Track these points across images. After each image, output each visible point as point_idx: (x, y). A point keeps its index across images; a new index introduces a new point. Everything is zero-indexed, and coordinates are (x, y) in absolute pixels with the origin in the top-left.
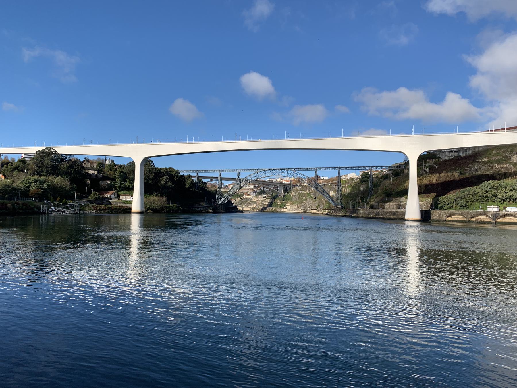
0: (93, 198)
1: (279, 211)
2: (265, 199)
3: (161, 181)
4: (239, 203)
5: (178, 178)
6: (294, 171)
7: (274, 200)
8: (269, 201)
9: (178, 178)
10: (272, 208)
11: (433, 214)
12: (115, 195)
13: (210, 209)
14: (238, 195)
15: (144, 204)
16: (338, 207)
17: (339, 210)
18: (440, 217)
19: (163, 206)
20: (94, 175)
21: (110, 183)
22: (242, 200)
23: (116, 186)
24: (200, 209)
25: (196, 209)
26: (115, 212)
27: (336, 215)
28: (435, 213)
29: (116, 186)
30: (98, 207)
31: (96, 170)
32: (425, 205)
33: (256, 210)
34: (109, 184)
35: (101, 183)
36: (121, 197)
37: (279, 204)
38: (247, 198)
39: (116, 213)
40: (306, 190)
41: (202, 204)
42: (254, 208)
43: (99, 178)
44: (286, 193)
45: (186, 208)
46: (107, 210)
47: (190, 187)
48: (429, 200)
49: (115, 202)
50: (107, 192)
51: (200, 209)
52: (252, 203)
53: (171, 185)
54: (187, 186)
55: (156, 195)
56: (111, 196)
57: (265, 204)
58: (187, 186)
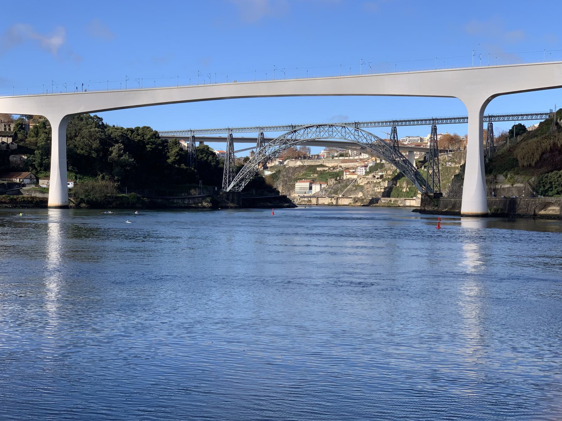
1: (401, 205)
2: (381, 180)
3: (112, 152)
4: (333, 191)
5: (154, 146)
7: (396, 183)
8: (386, 186)
9: (154, 146)
10: (389, 199)
11: (519, 205)
12: (31, 178)
13: (207, 202)
14: (336, 173)
15: (69, 193)
16: (429, 196)
17: (429, 200)
18: (527, 211)
19: (110, 197)
20: (5, 144)
21: (26, 158)
22: (340, 183)
23: (34, 163)
24: (186, 202)
25: (180, 201)
27: (425, 210)
28: (522, 202)
29: (34, 163)
31: (10, 136)
32: (525, 189)
33: (359, 204)
34: (24, 161)
35: (12, 158)
36: (41, 181)
37: (404, 190)
38: (348, 179)
39: (33, 207)
41: (193, 192)
42: (356, 200)
44: (421, 167)
45: (159, 200)
46: (8, 203)
47: (179, 162)
48: (533, 179)
49: (28, 191)
50: (19, 173)
51: (186, 202)
54: (169, 161)
55: (103, 178)
56: (25, 180)
57: (379, 191)
58: (169, 161)
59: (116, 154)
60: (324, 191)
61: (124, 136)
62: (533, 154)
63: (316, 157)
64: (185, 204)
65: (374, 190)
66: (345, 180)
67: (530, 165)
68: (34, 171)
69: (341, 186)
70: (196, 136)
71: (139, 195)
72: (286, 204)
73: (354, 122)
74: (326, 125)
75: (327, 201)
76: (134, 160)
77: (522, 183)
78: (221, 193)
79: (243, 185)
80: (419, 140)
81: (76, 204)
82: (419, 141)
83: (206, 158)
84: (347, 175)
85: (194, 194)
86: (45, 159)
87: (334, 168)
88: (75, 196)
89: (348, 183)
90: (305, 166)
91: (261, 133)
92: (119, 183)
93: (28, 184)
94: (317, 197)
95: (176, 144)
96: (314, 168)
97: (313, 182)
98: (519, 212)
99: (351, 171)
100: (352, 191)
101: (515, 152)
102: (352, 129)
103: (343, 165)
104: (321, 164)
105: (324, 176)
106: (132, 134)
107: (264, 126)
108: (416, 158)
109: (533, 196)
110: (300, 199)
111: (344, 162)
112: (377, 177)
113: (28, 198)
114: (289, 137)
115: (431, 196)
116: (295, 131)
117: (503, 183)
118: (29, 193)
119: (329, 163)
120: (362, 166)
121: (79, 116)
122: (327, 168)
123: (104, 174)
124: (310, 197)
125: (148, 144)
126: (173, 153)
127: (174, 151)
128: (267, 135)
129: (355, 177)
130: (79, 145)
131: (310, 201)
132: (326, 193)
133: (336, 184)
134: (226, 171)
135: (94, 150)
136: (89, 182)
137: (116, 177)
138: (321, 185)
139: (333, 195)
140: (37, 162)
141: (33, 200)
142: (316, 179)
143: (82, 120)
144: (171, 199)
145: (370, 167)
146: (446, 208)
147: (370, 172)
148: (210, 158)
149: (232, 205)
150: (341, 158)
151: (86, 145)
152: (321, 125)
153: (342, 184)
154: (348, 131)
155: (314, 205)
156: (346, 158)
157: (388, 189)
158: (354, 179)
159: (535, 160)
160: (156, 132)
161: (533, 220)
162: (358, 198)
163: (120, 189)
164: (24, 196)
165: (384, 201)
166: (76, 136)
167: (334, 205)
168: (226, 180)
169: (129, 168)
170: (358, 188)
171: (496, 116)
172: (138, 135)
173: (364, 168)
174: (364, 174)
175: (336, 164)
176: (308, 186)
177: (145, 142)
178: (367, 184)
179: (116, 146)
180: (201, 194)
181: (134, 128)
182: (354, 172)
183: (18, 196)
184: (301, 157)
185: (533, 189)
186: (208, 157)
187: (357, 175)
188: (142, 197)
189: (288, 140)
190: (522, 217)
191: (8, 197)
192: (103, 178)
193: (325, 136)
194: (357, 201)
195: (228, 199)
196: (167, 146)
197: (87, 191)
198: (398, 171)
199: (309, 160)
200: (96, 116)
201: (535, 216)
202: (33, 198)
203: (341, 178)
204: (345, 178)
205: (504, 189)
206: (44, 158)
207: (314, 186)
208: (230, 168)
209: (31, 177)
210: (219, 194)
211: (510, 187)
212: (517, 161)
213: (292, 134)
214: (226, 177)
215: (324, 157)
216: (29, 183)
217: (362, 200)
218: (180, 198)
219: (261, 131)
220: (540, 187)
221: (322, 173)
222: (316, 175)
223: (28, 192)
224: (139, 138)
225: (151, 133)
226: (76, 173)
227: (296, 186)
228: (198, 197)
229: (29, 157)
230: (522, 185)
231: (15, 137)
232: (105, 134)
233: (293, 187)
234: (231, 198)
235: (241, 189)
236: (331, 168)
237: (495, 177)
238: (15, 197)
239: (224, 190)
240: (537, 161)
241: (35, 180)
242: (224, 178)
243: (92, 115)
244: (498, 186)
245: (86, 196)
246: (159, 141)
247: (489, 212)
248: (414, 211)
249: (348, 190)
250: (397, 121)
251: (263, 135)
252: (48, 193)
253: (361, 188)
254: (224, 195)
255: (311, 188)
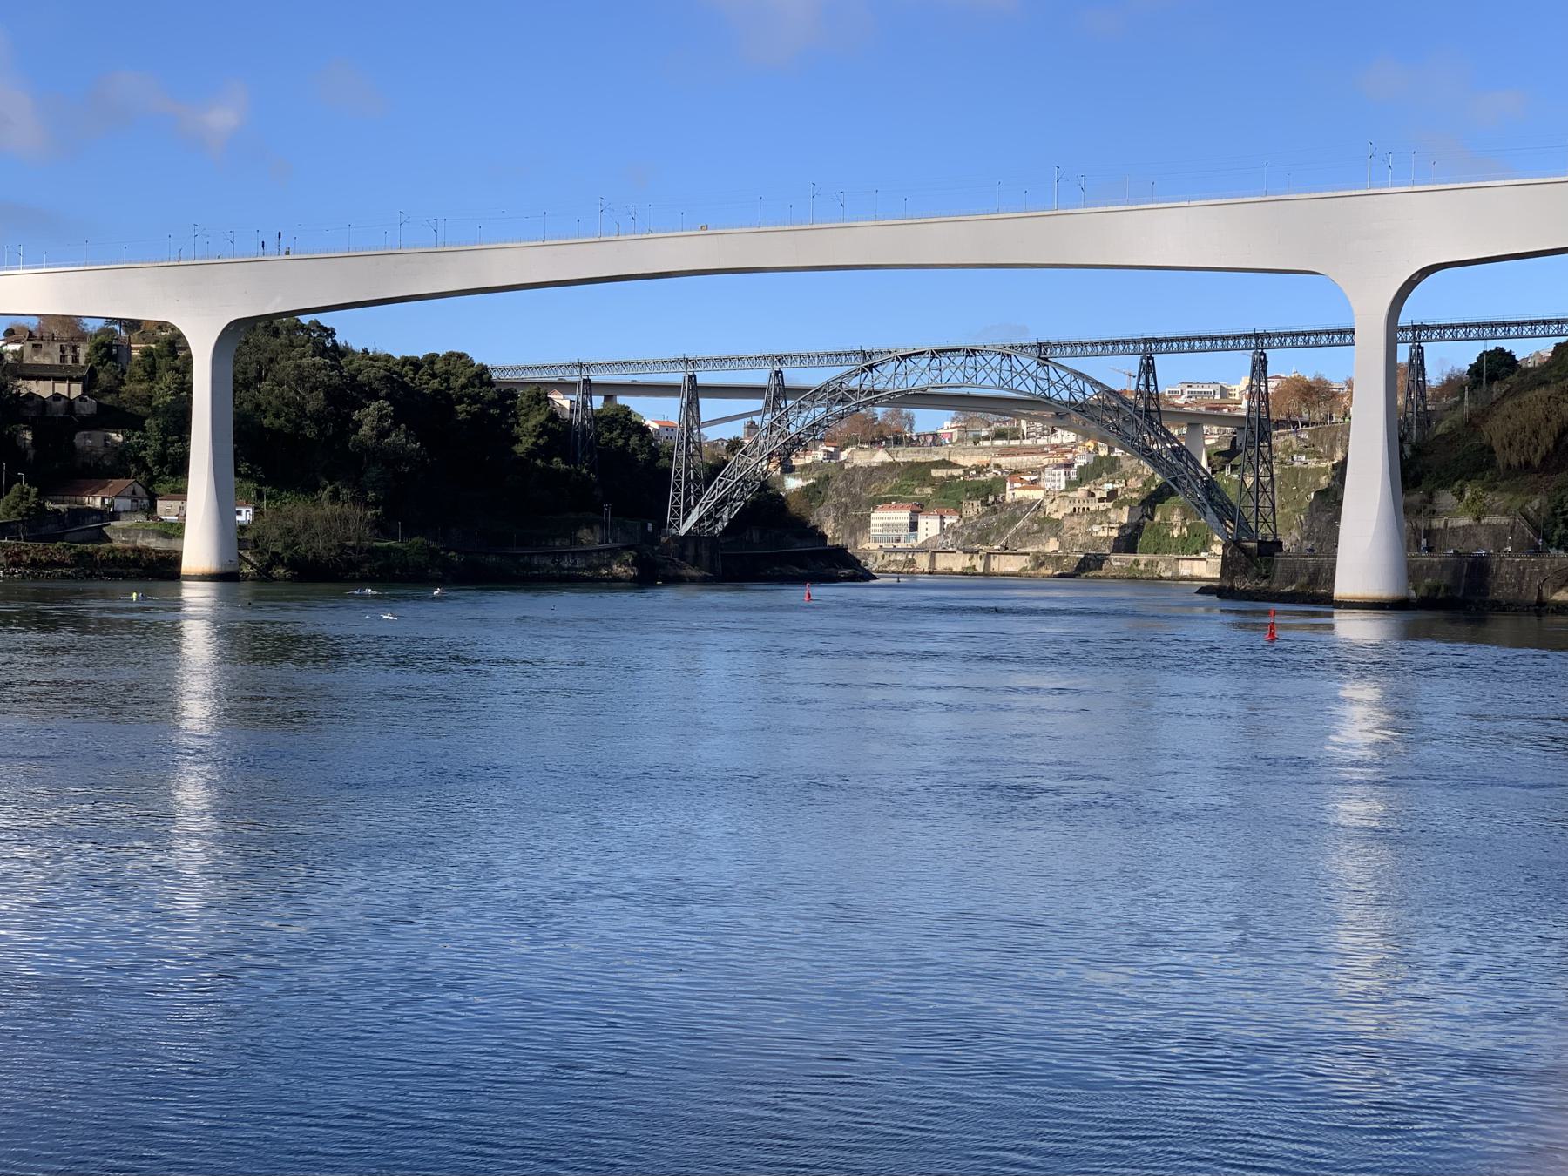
0: (14, 513)
1: (1168, 574)
2: (1109, 505)
3: (359, 424)
4: (975, 534)
5: (476, 408)
6: (1043, 361)
7: (1153, 513)
8: (1125, 520)
9: (476, 408)
10: (1132, 557)
12: (134, 497)
13: (625, 563)
14: (983, 484)
15: (236, 539)
16: (1244, 550)
18: (1521, 589)
19: (353, 548)
21: (120, 439)
22: (995, 511)
24: (566, 563)
25: (549, 562)
26: (107, 574)
27: (1232, 588)
28: (1505, 568)
30: (27, 553)
31: (77, 379)
32: (1512, 532)
33: (1049, 572)
35: (83, 440)
36: (161, 505)
37: (1176, 533)
38: (1019, 502)
40: (1332, 448)
41: (584, 534)
42: (1040, 560)
43: (82, 418)
44: (1223, 469)
46: (72, 566)
47: (545, 452)
48: (1536, 503)
49: (125, 531)
52: (1040, 531)
53: (403, 446)
54: (520, 449)
55: (335, 496)
56: (117, 501)
57: (1102, 534)
58: (520, 449)
59: (372, 430)
60: (950, 535)
61: (396, 381)
62: (1535, 433)
63: (930, 439)
64: (564, 569)
65: (1092, 532)
66: (1009, 505)
67: (1528, 464)
68: (143, 475)
69: (999, 520)
70: (594, 379)
71: (434, 545)
72: (846, 572)
73: (1035, 343)
74: (959, 350)
75: (958, 562)
76: (421, 446)
77: (1505, 513)
78: (664, 540)
79: (725, 517)
80: (1218, 392)
81: (258, 569)
82: (1218, 397)
83: (621, 442)
84: (1016, 491)
85: (589, 543)
86: (173, 443)
87: (979, 470)
88: (257, 547)
89: (1018, 512)
90: (899, 463)
91: (777, 373)
92: (379, 511)
93: (125, 511)
94: (930, 550)
95: (538, 403)
96: (923, 468)
97: (919, 508)
98: (1498, 594)
99: (1027, 478)
100: (1028, 534)
101: (1485, 429)
102: (1028, 362)
103: (1005, 462)
104: (944, 460)
105: (951, 493)
106: (416, 373)
107: (785, 353)
108: (1208, 442)
109: (1537, 551)
110: (883, 557)
111: (1008, 455)
112: (1098, 495)
113: (125, 550)
114: (854, 383)
115: (1251, 549)
116: (871, 367)
117: (1453, 514)
118: (128, 537)
119: (964, 456)
120: (1058, 466)
121: (269, 324)
122: (961, 472)
123: (337, 484)
124: (913, 551)
125: (460, 402)
126: (531, 428)
127: (532, 422)
128: (796, 376)
129: (1037, 495)
130: (270, 403)
131: (912, 562)
132: (957, 539)
133: (985, 514)
134: (679, 477)
135: (310, 418)
136: (296, 508)
137: (372, 494)
138: (942, 518)
139: (976, 547)
140: (150, 452)
141: (140, 555)
142: (928, 501)
143: (276, 333)
144: (524, 555)
145: (1079, 467)
146: (1291, 584)
147: (1081, 481)
148: (634, 440)
149: (693, 572)
150: (998, 443)
151: (287, 405)
152: (943, 351)
153: (1003, 516)
154: (1019, 368)
155: (923, 572)
156: (1013, 443)
157: (1130, 531)
158: (1035, 501)
159: (1541, 450)
160: (484, 368)
161: (1534, 619)
162: (1045, 555)
163: (382, 528)
164: (114, 544)
165: (1118, 562)
166: (260, 379)
167: (980, 574)
168: (677, 503)
169: (407, 470)
170: (1046, 526)
171: (1433, 328)
172: (434, 376)
173: (1062, 471)
174: (1063, 486)
175: (985, 459)
176: (908, 521)
177: (451, 395)
178: (1071, 515)
179: (371, 408)
180: (607, 542)
181: (421, 357)
182: (1034, 482)
183: (96, 546)
184: (886, 440)
185: (1536, 530)
186: (627, 440)
187: (1043, 489)
188: (442, 549)
189: (851, 392)
190: (1504, 610)
191: (71, 547)
192: (335, 496)
193: (953, 381)
194: (1042, 564)
195: (682, 557)
196: (513, 406)
197: (289, 531)
198: (1159, 478)
199: (910, 449)
200: (317, 323)
201: (1541, 607)
202: (138, 551)
203: (1000, 499)
204: (1009, 498)
205: (1454, 530)
206: (170, 439)
207: (922, 522)
208: (688, 468)
209: (134, 492)
210: (657, 542)
211: (1470, 526)
212: (1492, 451)
213: (864, 375)
214: (677, 495)
215: (950, 439)
216: (128, 508)
217: (1056, 559)
218: (548, 554)
219: (777, 366)
220: (1556, 526)
221: (945, 485)
222: (929, 490)
223: (128, 533)
224: (436, 385)
225: (470, 372)
226: (261, 482)
227: (873, 522)
228: (599, 551)
229: (128, 438)
230: (1504, 520)
231: (89, 382)
232: (341, 373)
233: (865, 523)
234: (690, 552)
235: (720, 529)
236: (971, 469)
237: (1431, 498)
238: (90, 547)
239: (673, 531)
240: (1548, 452)
241: (146, 501)
242: (673, 499)
243: (305, 320)
244: (1438, 523)
245: (287, 547)
246: (491, 394)
247: (1413, 594)
248: (1202, 591)
249: (1017, 533)
250: (1156, 341)
251: (782, 377)
252: (181, 536)
253: (1055, 527)
254: (672, 544)
255: (914, 526)
